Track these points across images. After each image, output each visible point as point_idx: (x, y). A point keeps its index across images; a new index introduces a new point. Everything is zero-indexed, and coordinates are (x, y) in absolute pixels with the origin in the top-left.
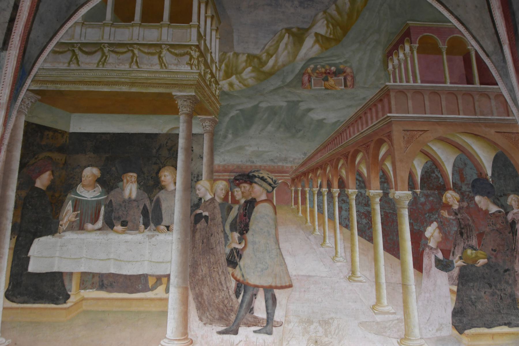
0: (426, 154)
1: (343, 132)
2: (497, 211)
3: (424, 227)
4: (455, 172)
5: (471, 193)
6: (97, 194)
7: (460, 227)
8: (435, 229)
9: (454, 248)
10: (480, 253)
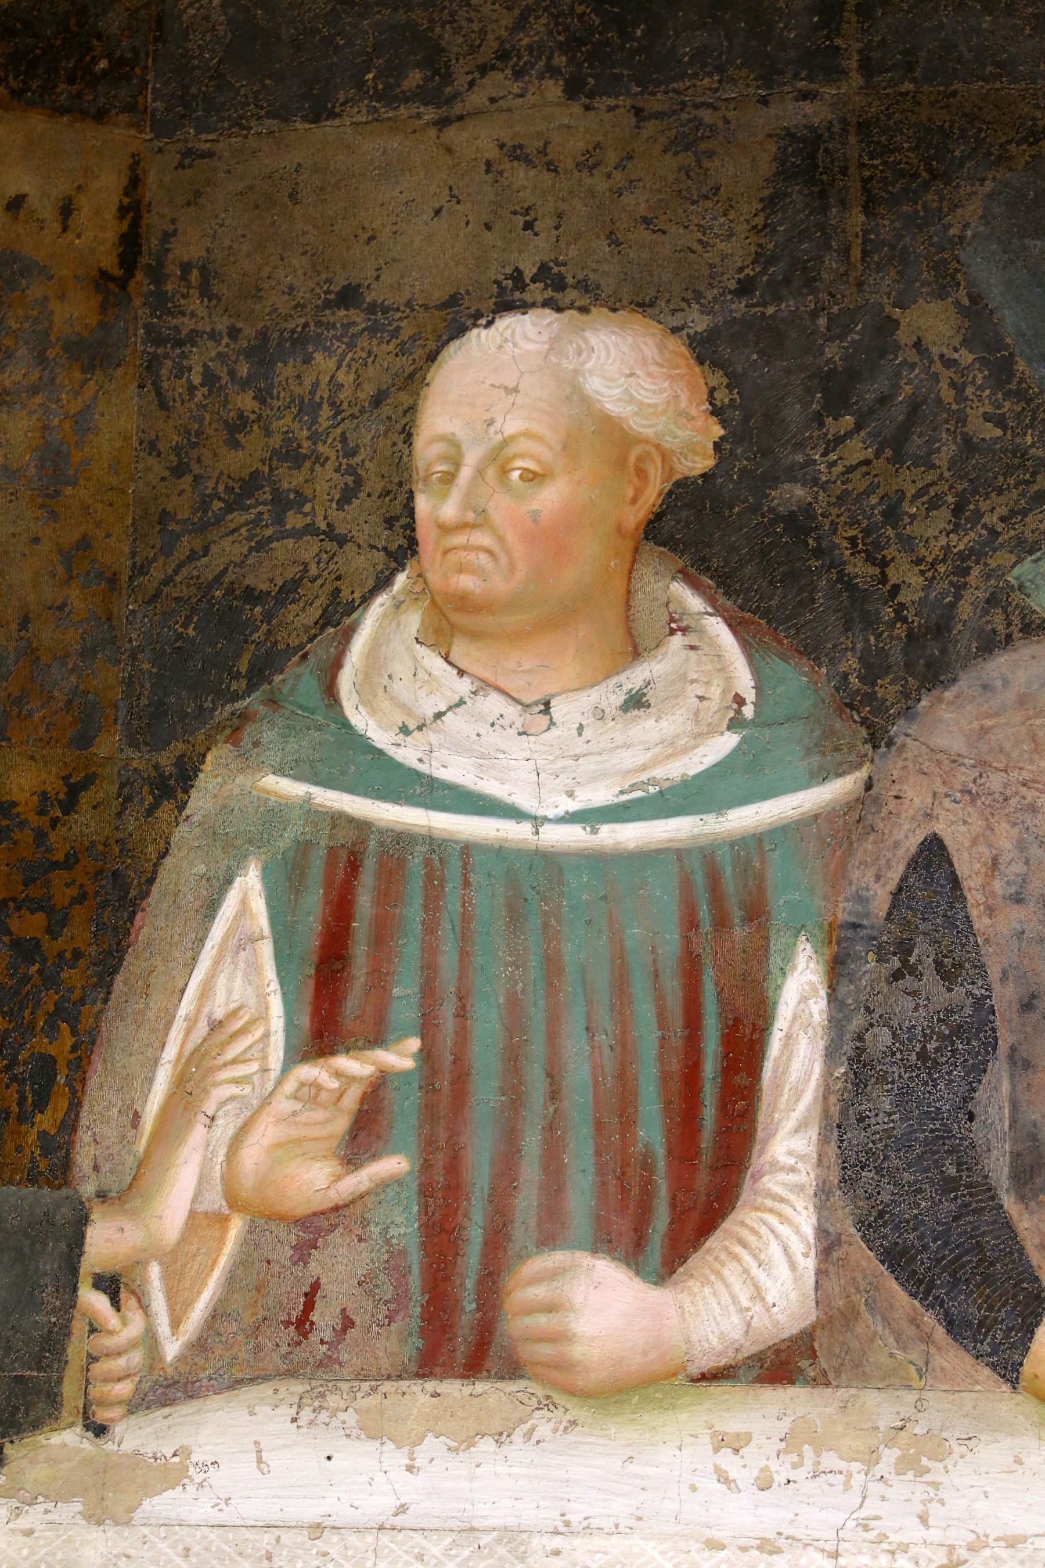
6: (673, 749)
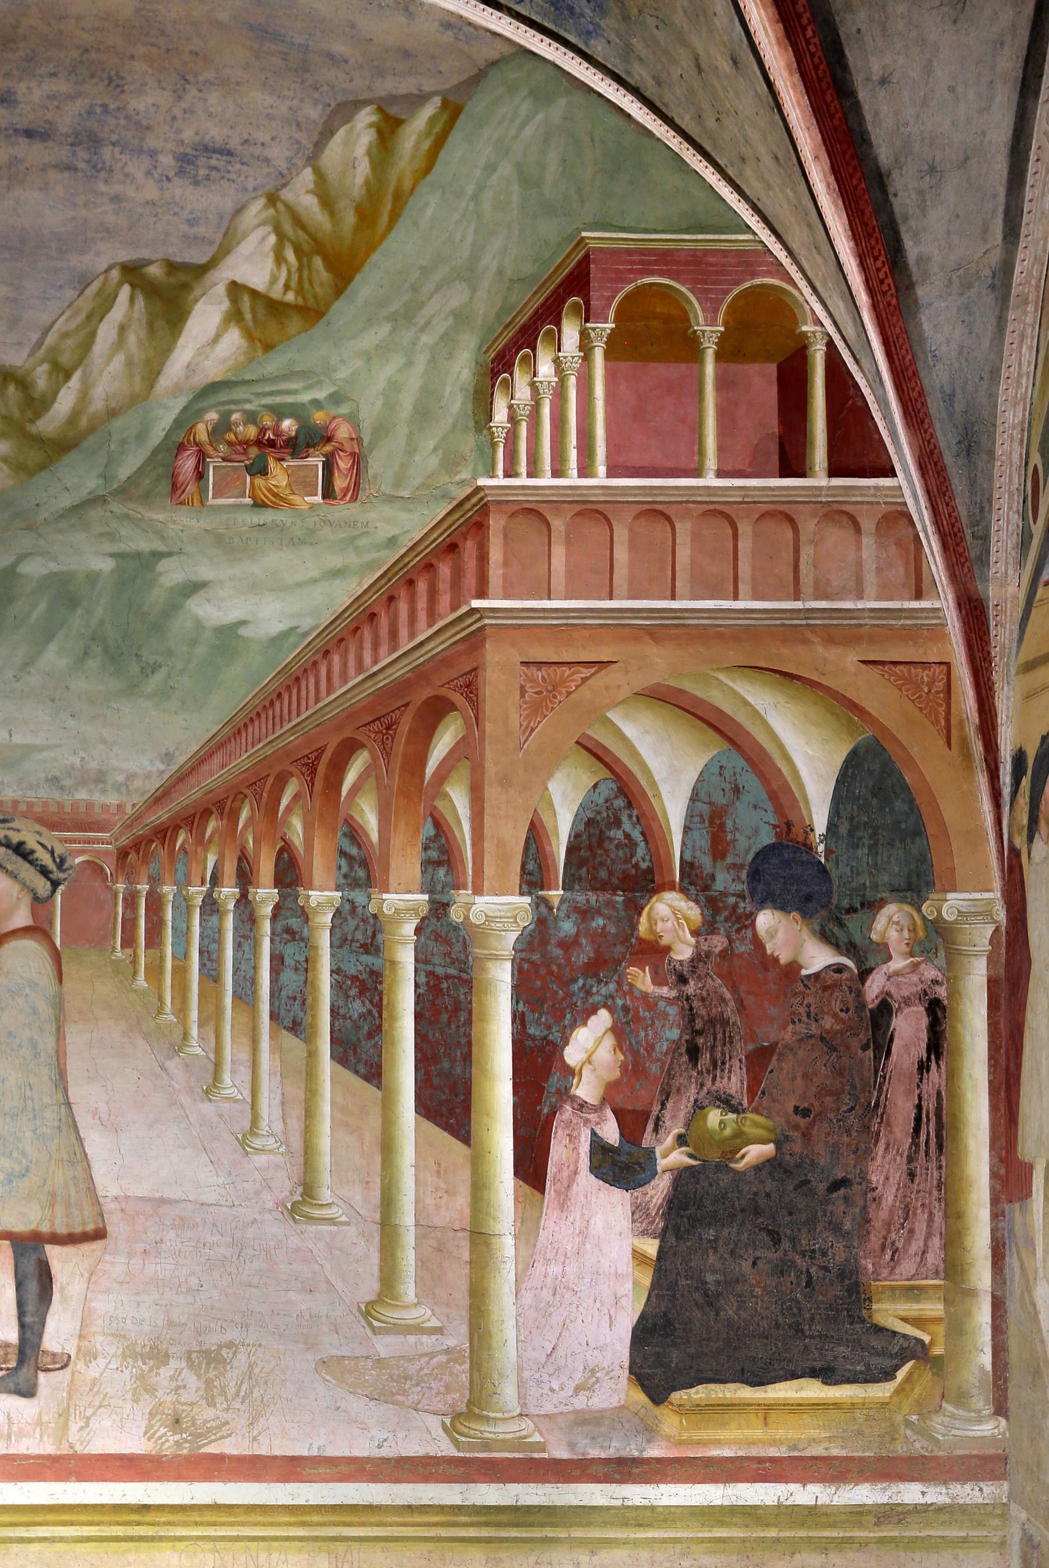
0: (597, 753)
1: (305, 671)
2: (829, 966)
3: (565, 1027)
4: (697, 819)
5: (744, 898)
7: (692, 1027)
9: (663, 1105)
10: (754, 1122)
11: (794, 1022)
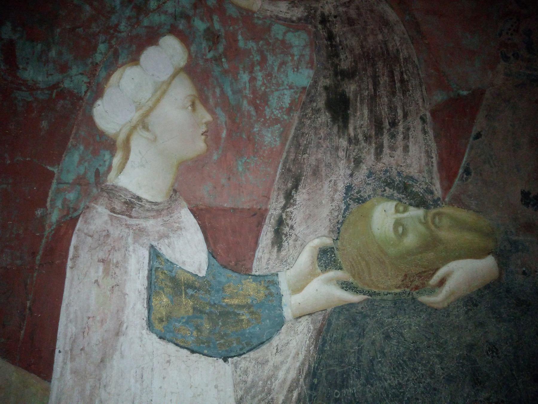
7: (335, 66)
8: (169, 83)
9: (289, 196)
11: (506, 58)
